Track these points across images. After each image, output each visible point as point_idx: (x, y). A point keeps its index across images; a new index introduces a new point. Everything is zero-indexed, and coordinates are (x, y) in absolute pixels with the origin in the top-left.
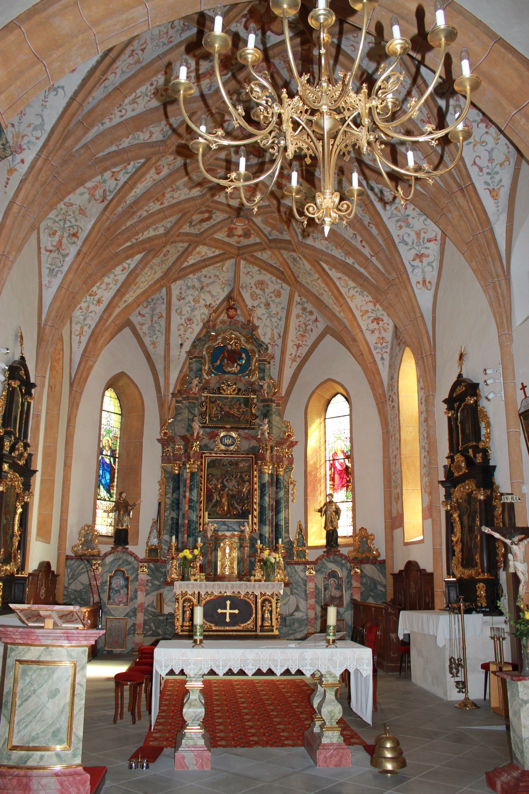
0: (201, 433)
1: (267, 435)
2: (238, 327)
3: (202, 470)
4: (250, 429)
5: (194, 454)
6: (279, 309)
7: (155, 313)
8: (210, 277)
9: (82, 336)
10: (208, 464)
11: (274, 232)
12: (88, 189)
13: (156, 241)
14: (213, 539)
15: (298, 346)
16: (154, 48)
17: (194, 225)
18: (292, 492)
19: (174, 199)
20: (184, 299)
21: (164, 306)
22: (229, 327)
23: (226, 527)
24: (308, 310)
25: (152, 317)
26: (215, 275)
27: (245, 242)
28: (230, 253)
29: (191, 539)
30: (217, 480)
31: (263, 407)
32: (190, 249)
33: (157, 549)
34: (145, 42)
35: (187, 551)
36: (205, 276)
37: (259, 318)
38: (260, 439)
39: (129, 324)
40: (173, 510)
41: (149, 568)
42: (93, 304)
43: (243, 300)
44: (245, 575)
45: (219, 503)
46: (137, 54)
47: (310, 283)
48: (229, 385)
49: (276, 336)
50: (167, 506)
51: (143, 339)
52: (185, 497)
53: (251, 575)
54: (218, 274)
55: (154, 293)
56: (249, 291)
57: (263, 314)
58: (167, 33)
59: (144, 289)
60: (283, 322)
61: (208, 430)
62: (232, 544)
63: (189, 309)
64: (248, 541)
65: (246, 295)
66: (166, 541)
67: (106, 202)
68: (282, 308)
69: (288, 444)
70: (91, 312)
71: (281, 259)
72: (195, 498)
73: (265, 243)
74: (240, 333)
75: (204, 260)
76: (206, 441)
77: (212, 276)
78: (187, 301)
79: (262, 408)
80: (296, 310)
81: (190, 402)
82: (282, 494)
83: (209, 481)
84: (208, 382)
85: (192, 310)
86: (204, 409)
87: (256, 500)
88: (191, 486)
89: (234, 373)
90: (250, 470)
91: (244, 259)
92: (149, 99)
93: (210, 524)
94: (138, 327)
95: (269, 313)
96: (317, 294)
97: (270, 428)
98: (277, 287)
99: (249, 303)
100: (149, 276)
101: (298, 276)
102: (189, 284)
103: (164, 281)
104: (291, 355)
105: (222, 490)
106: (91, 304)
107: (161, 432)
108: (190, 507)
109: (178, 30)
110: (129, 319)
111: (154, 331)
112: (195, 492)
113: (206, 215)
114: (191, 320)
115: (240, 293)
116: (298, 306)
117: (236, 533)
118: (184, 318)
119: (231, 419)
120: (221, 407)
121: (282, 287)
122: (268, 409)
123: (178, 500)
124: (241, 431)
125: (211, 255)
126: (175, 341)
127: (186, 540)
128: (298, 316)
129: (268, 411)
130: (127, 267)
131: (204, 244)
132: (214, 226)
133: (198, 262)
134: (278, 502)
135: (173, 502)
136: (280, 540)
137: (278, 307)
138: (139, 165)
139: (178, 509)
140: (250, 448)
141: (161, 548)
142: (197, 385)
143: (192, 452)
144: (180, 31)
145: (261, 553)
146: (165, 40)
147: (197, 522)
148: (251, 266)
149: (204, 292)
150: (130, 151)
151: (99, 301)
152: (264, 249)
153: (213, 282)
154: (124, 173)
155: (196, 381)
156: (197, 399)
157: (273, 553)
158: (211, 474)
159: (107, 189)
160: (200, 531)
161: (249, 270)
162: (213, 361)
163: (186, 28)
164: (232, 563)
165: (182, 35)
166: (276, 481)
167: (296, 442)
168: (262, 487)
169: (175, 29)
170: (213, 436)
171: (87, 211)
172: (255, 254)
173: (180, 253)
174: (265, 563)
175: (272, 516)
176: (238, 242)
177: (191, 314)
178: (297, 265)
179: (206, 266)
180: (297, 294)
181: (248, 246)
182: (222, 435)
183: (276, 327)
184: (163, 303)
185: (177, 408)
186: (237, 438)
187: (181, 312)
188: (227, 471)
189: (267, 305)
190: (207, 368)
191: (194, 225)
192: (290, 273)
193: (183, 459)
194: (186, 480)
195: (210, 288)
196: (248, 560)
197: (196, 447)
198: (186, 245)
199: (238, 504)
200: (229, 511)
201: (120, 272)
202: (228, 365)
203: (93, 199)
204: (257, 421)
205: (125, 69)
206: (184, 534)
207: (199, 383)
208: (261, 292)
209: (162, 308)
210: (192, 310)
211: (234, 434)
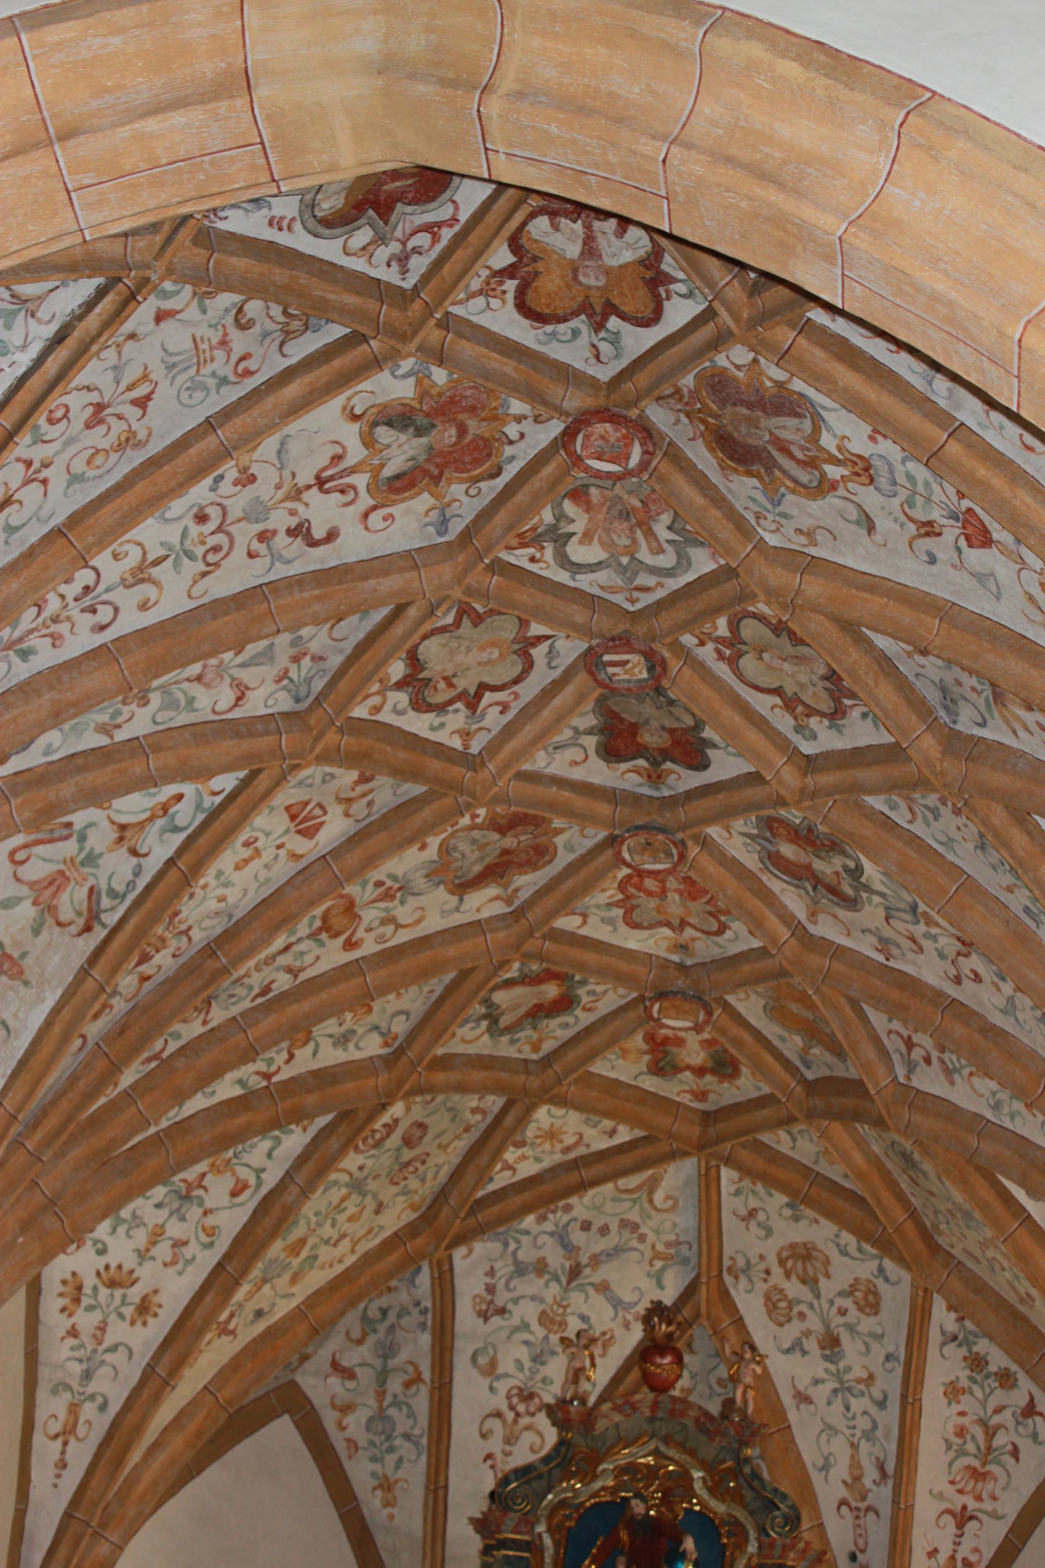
2: (685, 1427)
7: (391, 1363)
8: (604, 1230)
9: (72, 1441)
11: (816, 1051)
12: (32, 885)
13: (350, 1085)
15: (963, 1518)
16: (184, 396)
17: (508, 1029)
19: (399, 926)
20: (502, 1311)
21: (425, 1339)
22: (647, 1427)
24: (993, 1368)
25: (382, 1378)
26: (624, 1224)
27: (727, 1093)
28: (670, 1135)
32: (509, 1120)
34: (145, 377)
36: (586, 1226)
37: (802, 1398)
39: (293, 1402)
42: (121, 1316)
43: (739, 1322)
46: (120, 417)
47: (977, 1252)
49: (870, 1474)
51: (347, 1465)
54: (634, 1216)
55: (382, 1285)
56: (761, 1287)
57: (816, 1382)
58: (224, 343)
59: (339, 1269)
60: (890, 1418)
63: (523, 1353)
65: (749, 1302)
67: (100, 934)
68: (888, 1357)
70: (114, 1348)
71: (858, 1158)
73: (790, 1096)
74: (692, 1453)
75: (576, 1164)
77: (614, 1228)
78: (515, 1321)
80: (943, 1367)
85: (538, 1359)
91: (729, 1161)
92: (201, 567)
94: (329, 1418)
95: (838, 1376)
96: (1012, 1298)
98: (865, 1270)
100: (351, 1219)
101: (935, 1227)
102: (521, 1255)
103: (420, 1241)
106: (113, 1318)
109: (265, 335)
110: (293, 1385)
111: (389, 1438)
113: (551, 991)
115: (725, 1295)
116: (950, 1349)
121: (881, 1270)
125: (604, 1144)
128: (953, 1392)
130: (252, 1181)
131: (561, 1101)
132: (589, 1031)
133: (552, 1172)
138: (218, 799)
144: (279, 337)
146: (221, 365)
148: (759, 1187)
149: (581, 1288)
150: (157, 748)
151: (144, 1308)
152: (789, 1121)
153: (618, 1251)
154: (164, 831)
159: (104, 886)
161: (753, 1203)
163: (296, 325)
165: (286, 349)
169: (256, 330)
171: (28, 962)
172: (766, 1138)
173: (475, 1135)
176: (702, 1095)
177: (533, 1372)
178: (921, 1180)
179: (581, 1187)
181: (736, 1109)
183: (869, 1435)
184: (423, 1326)
187: (493, 1364)
189: (831, 1343)
191: (508, 1029)
192: (901, 1216)
195: (606, 1272)
198: (494, 1102)
201: (226, 1201)
203: (50, 921)
205: (79, 466)
210: (538, 1359)
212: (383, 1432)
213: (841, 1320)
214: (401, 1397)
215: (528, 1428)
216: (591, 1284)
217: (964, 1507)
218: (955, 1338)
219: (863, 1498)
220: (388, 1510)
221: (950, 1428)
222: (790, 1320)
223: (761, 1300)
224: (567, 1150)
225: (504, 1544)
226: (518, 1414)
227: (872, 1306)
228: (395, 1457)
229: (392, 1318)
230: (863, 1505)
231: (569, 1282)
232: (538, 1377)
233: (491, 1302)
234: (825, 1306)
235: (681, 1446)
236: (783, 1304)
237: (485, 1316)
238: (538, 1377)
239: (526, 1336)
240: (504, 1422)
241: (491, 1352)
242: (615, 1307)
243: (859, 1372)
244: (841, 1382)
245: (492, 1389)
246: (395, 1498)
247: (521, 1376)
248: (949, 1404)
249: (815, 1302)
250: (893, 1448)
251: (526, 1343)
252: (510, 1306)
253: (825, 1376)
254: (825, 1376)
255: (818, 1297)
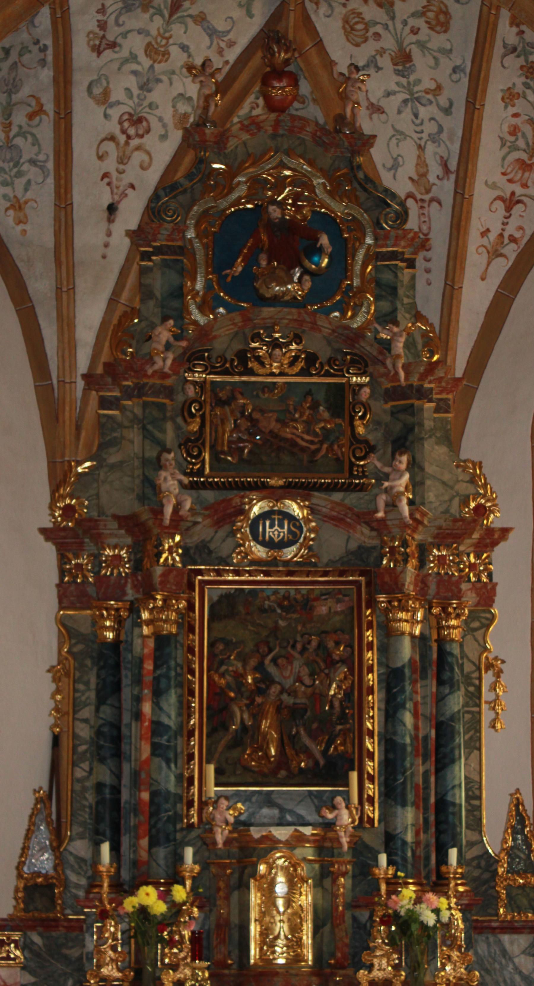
0: (188, 505)
1: (405, 510)
3: (191, 630)
4: (349, 488)
5: (165, 575)
6: (443, 74)
7: (15, 98)
10: (211, 608)
14: (234, 850)
15: (510, 203)
18: (492, 696)
20: (113, 45)
21: (46, 75)
23: (276, 812)
29: (161, 853)
30: (243, 659)
31: (393, 413)
33: (51, 887)
35: (150, 889)
37: (376, 109)
38: (383, 521)
40: (102, 760)
41: (24, 946)
43: (319, 44)
44: (340, 966)
45: (249, 735)
48: (275, 344)
49: (435, 170)
50: (82, 748)
52: (138, 715)
53: (359, 965)
56: (340, 11)
60: (456, 123)
61: (209, 496)
62: (295, 866)
63: (132, 82)
64: (348, 858)
66: (81, 860)
68: (455, 70)
69: (476, 536)
72: (171, 719)
76: (203, 531)
78: (125, 53)
79: (387, 418)
81: (145, 405)
82: (456, 702)
83: (216, 661)
84: (204, 333)
85: (145, 87)
86: (195, 427)
87: (373, 722)
88: (157, 680)
89: (293, 302)
90: (352, 623)
93: (224, 803)
97: (416, 484)
99: (341, 53)
104: (485, 233)
105: (260, 692)
107: (52, 507)
108: (156, 749)
112: (171, 701)
114: (140, 120)
116: (510, 60)
117: (308, 831)
118: (115, 113)
119: (286, 458)
120: (250, 418)
122: (410, 419)
123: (117, 726)
124: (319, 498)
126: (88, 196)
127: (144, 855)
128: (510, 97)
129: (409, 429)
134: (444, 729)
135: (99, 733)
136: (453, 853)
137: (439, 68)
139: (118, 755)
140: (349, 553)
141: (65, 884)
142: (168, 346)
143: (159, 571)
145: (389, 893)
147: (180, 798)
149: (182, 21)
155: (163, 334)
156: (170, 392)
157: (430, 896)
158: (222, 640)
160: (191, 826)
162: (219, 264)
164: (295, 929)
166: (439, 662)
167: (505, 532)
168: (393, 679)
170: (227, 515)
174: (405, 928)
175: (426, 775)
177: (141, 99)
180: (505, 15)
182: (256, 510)
183: (433, 138)
184: (43, 63)
185: (103, 425)
186: (307, 521)
187: (106, 93)
188: (276, 628)
189: (403, 60)
190: (199, 286)
193: (131, 594)
194: (141, 661)
196: (348, 916)
197: (170, 553)
199: (313, 736)
200: (283, 760)
202: (272, 276)
204: (374, 462)
206: (138, 838)
207: (177, 337)
208: (380, 15)
209: (40, 81)
210: (145, 87)
211: (295, 508)
212: (12, 159)
213: (414, 38)
214: (26, 128)
215: (138, 148)
216: (190, 16)
217: (513, 194)
218: (514, 49)
219: (428, 191)
220: (20, 227)
221: (505, 128)
222: (366, 40)
223: (340, 23)
226: (129, 137)
227: (442, 25)
228: (24, 180)
229: (14, 56)
230: (427, 197)
231: (171, 16)
232: (146, 103)
233: (104, 37)
234: (399, 26)
236: (360, 27)
237: (98, 50)
238: (146, 103)
239: (135, 67)
240: (118, 144)
241: (105, 84)
242: (210, 36)
243: (428, 84)
244: (411, 93)
245: (106, 116)
246: (26, 217)
247: (131, 103)
248: (506, 107)
249: (390, 23)
250: (456, 147)
251: (135, 73)
252: (119, 40)
253: (397, 89)
254: (397, 89)
255: (393, 18)
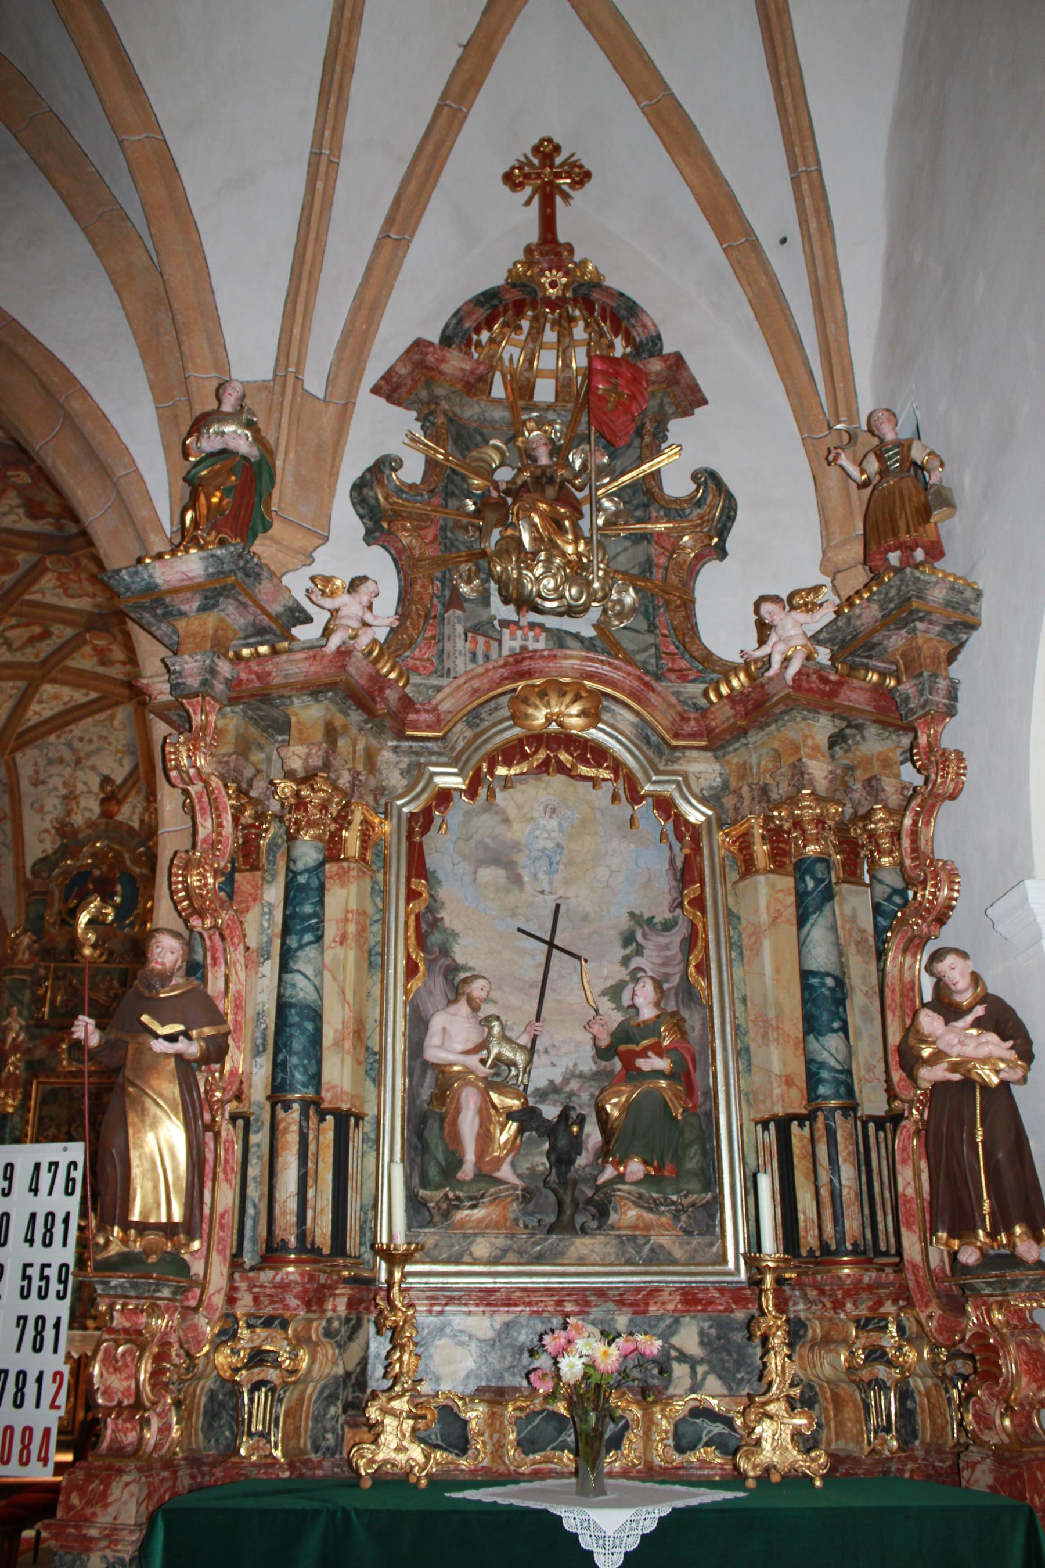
8: (91, 741)
20: (43, 782)
26: (101, 737)
36: (81, 739)
54: (104, 733)
63: (57, 802)
77: (95, 739)
78: (51, 786)
102: (50, 755)
113: (37, 630)
118: (48, 818)
125: (84, 700)
131: (54, 681)
149: (83, 769)
179: (75, 721)
195: (94, 760)
198: (21, 684)
224: (66, 704)
225: (35, 893)
235: (121, 844)
237: (35, 785)
